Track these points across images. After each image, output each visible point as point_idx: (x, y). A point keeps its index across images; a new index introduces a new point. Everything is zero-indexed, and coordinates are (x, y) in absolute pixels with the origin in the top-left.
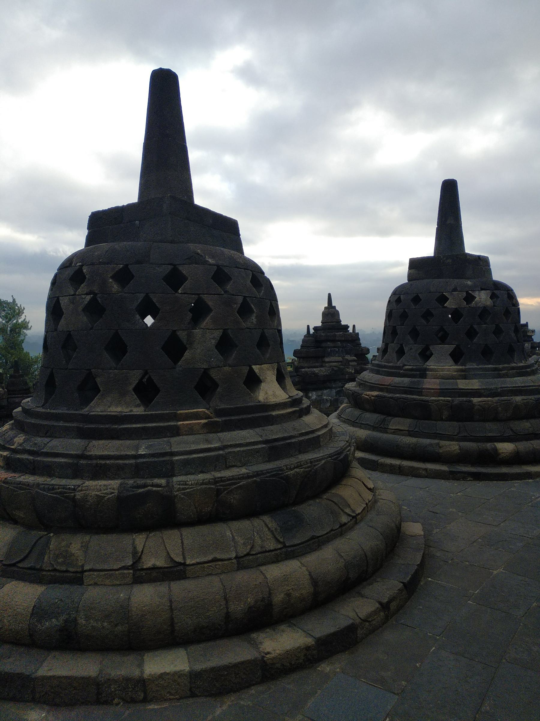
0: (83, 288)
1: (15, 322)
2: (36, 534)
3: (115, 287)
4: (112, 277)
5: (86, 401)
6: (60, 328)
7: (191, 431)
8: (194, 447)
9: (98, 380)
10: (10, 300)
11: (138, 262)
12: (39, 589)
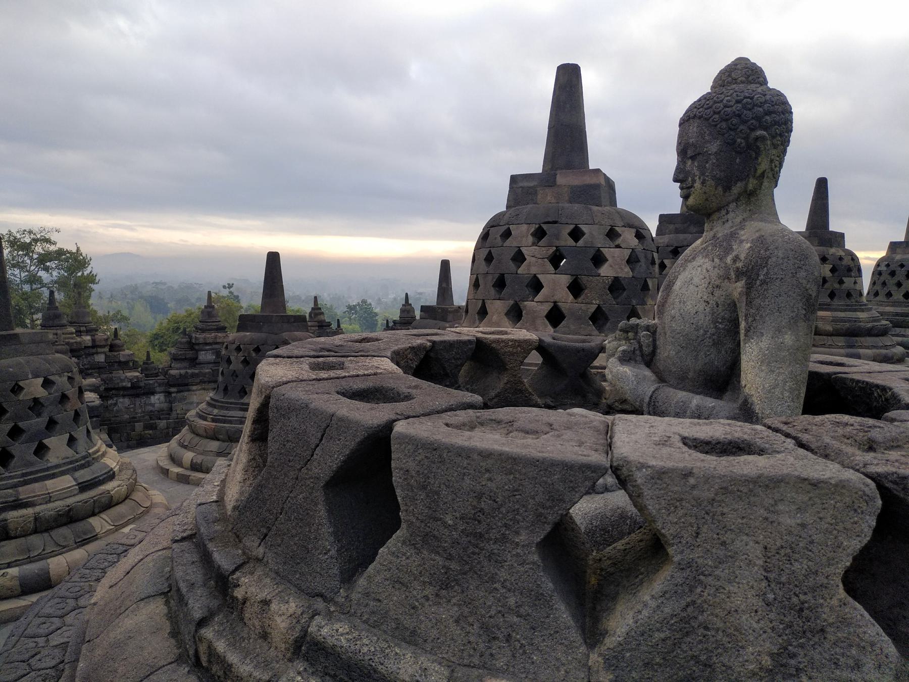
0: (241, 354)
1: (79, 274)
2: (226, 444)
3: (254, 354)
4: (253, 350)
5: (242, 397)
6: (230, 368)
9: (247, 389)
10: (74, 250)
11: (263, 345)
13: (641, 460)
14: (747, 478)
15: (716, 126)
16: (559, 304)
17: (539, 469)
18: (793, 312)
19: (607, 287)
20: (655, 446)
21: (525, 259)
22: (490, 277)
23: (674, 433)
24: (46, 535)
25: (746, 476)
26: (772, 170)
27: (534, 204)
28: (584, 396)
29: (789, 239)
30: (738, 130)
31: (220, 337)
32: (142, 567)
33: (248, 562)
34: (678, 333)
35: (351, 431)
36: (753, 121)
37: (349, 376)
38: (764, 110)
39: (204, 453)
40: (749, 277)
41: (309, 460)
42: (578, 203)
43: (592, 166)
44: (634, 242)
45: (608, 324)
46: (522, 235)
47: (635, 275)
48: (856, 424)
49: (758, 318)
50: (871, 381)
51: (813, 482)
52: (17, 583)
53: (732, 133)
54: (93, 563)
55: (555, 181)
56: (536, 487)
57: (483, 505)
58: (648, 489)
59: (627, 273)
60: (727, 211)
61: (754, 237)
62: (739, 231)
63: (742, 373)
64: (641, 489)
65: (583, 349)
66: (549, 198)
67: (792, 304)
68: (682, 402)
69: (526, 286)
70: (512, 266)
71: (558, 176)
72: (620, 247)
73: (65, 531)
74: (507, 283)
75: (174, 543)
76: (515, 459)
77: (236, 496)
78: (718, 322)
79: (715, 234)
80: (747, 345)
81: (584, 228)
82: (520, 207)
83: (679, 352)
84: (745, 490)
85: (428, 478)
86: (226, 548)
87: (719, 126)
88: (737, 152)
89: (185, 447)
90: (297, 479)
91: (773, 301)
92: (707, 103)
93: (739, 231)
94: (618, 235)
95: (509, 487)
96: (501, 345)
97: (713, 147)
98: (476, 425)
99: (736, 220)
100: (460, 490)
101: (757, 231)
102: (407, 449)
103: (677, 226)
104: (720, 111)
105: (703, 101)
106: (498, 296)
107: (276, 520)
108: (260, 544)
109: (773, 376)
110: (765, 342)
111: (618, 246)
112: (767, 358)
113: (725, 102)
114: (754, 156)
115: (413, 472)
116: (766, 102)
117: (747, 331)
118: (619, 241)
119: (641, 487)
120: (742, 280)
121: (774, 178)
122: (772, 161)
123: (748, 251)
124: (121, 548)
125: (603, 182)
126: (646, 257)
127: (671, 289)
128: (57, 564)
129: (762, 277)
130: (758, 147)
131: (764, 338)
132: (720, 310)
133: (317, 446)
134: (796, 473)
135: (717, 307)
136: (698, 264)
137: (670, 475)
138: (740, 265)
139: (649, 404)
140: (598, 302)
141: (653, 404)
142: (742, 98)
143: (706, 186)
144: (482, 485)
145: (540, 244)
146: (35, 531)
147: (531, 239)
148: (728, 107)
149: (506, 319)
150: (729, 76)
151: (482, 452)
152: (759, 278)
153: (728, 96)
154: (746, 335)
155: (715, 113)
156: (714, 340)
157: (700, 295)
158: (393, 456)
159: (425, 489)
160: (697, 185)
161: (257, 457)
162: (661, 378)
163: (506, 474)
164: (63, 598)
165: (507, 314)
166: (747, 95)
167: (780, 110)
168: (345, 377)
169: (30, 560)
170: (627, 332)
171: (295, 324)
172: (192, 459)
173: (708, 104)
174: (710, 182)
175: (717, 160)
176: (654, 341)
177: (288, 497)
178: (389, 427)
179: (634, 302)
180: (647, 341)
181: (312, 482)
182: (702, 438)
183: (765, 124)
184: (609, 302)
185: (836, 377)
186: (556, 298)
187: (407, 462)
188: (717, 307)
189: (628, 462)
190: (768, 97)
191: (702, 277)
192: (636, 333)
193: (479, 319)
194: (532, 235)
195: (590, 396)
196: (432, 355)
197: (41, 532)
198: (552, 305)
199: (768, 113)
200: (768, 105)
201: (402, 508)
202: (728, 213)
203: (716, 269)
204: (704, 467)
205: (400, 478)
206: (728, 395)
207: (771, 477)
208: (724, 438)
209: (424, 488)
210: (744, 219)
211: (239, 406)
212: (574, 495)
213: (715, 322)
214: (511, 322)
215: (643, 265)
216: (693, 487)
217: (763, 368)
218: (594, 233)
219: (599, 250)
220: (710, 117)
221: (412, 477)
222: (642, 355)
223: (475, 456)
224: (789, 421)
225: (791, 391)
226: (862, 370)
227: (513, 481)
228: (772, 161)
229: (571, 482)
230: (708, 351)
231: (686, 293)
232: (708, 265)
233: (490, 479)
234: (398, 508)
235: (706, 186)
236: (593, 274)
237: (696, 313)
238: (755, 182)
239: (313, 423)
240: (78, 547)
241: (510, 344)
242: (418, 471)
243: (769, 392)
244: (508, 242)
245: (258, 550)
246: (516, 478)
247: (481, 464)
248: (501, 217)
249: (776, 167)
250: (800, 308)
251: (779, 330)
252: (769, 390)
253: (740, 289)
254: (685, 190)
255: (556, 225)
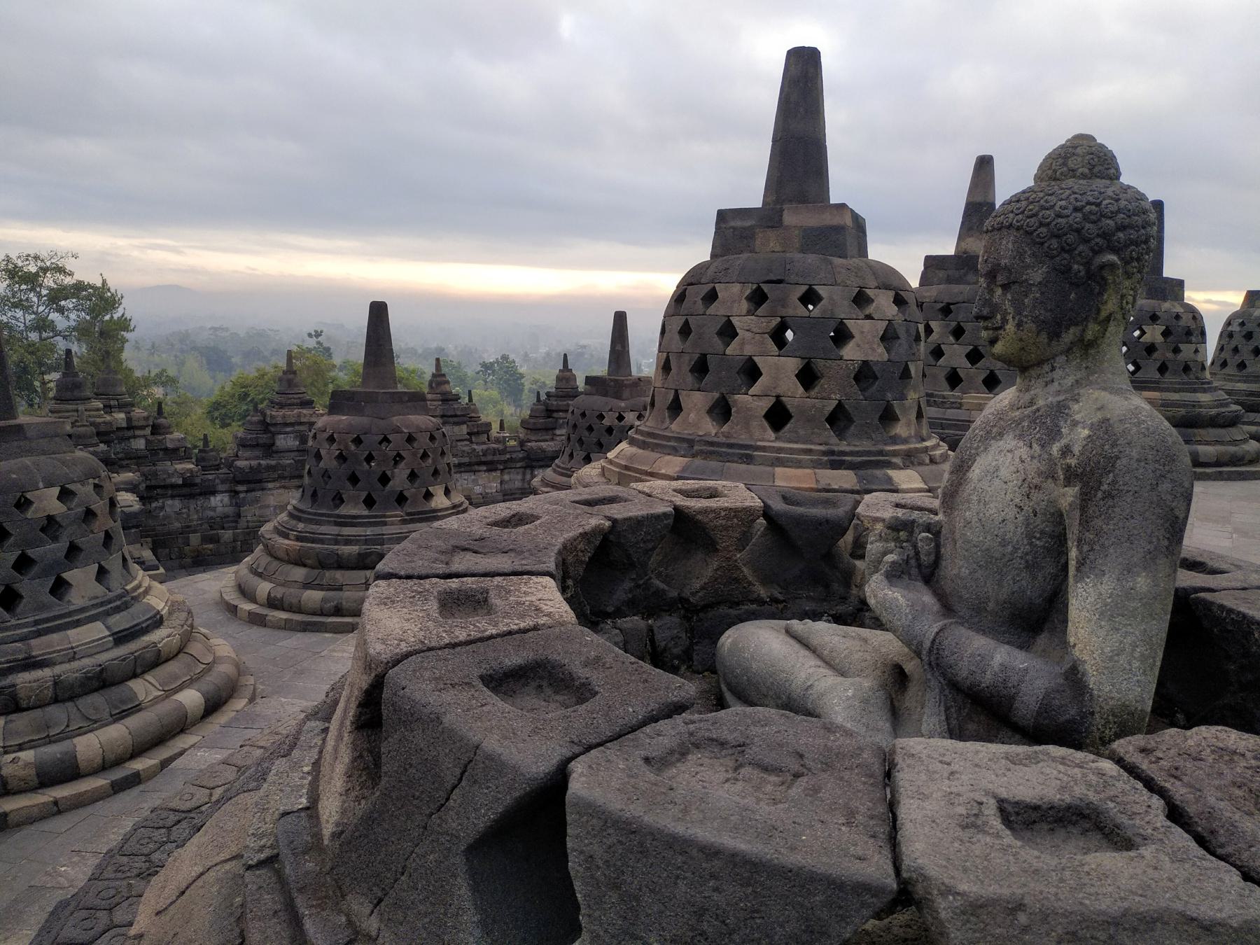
1: (107, 318)
2: (316, 571)
3: (353, 447)
4: (352, 441)
5: (337, 507)
7: (392, 523)
8: (394, 532)
9: (343, 496)
10: (99, 284)
12: (323, 593)
13: (947, 881)
14: (1105, 918)
15: (1042, 244)
16: (783, 399)
17: (792, 883)
18: (1150, 543)
19: (852, 375)
20: (959, 832)
21: (737, 334)
22: (686, 358)
23: (987, 793)
24: (69, 704)
25: (1104, 913)
26: (1122, 309)
27: (751, 252)
28: (827, 586)
29: (1148, 429)
30: (1077, 252)
31: (305, 415)
32: (201, 892)
33: (355, 940)
34: (976, 547)
35: (505, 779)
36: (1098, 240)
37: (498, 635)
38: (1116, 223)
39: (284, 584)
40: (1085, 485)
41: (442, 805)
42: (814, 253)
43: (834, 200)
44: (892, 310)
45: (852, 428)
46: (733, 298)
47: (892, 358)
48: (1248, 755)
49: (1097, 547)
50: (1251, 613)
51: (1205, 923)
52: (33, 772)
53: (1066, 256)
54: (132, 846)
55: (781, 220)
56: (786, 909)
57: (705, 926)
58: (957, 929)
59: (880, 355)
60: (1053, 367)
61: (1095, 420)
62: (1070, 404)
63: (1070, 624)
64: (946, 927)
65: (827, 521)
66: (772, 244)
67: (1149, 531)
68: (979, 655)
69: (738, 373)
70: (717, 342)
71: (785, 213)
72: (873, 319)
73: (97, 699)
74: (711, 367)
75: (247, 869)
76: (754, 864)
77: (335, 818)
78: (1035, 537)
79: (1032, 399)
80: (1079, 585)
81: (822, 291)
82: (733, 257)
83: (975, 571)
84: (1102, 936)
85: (623, 872)
86: (323, 910)
87: (1046, 245)
88: (1071, 284)
89: (260, 575)
90: (425, 828)
91: (1121, 524)
92: (1030, 207)
93: (1070, 404)
94: (869, 301)
95: (746, 905)
96: (710, 516)
97: (1037, 275)
98: (689, 749)
99: (1066, 381)
100: (671, 900)
101: (1099, 409)
102: (591, 823)
103: (950, 272)
104: (1049, 224)
105: (1024, 203)
106: (697, 386)
107: (396, 880)
108: (372, 912)
109: (1117, 636)
110: (1107, 586)
111: (869, 317)
112: (1109, 610)
113: (1057, 208)
114: (1097, 291)
115: (600, 861)
116: (1119, 211)
117: (1081, 564)
118: (870, 309)
119: (946, 924)
120: (1076, 486)
121: (1124, 319)
122: (1123, 297)
123: (1085, 443)
124: (173, 818)
125: (848, 221)
126: (907, 331)
127: (965, 474)
128: (88, 746)
129: (1105, 487)
130: (1103, 278)
131: (1105, 579)
132: (1038, 521)
133: (454, 787)
134: (1179, 906)
135: (1035, 516)
136: (1009, 447)
137: (990, 909)
138: (1073, 462)
139: (930, 651)
140: (838, 397)
141: (935, 652)
142: (1083, 204)
143: (1022, 330)
144: (705, 897)
145: (758, 312)
146: (56, 700)
147: (745, 305)
148: (1062, 217)
149: (708, 419)
150: (1064, 164)
151: (705, 847)
152: (1102, 488)
153: (1061, 200)
154: (1078, 569)
155: (1041, 225)
156: (1027, 562)
157: (1009, 497)
158: (569, 831)
159: (619, 888)
160: (1010, 327)
161: (365, 754)
162: (947, 608)
163: (742, 885)
164: (91, 909)
165: (710, 411)
166: (1091, 199)
167: (1140, 223)
168: (491, 637)
169: (50, 740)
170: (898, 531)
171: (409, 404)
172: (269, 592)
173: (1031, 210)
174: (1031, 326)
175: (1042, 293)
176: (938, 546)
177: (413, 852)
178: (560, 778)
179: (889, 396)
180: (927, 548)
181: (447, 841)
182: (1028, 800)
183: (1116, 244)
184: (854, 397)
185: (1198, 598)
186: (779, 391)
187: (591, 844)
188: (1035, 516)
189: (926, 878)
190: (1123, 203)
191: (1013, 469)
192: (911, 533)
193: (669, 417)
194: (746, 298)
195: (835, 586)
196: (612, 537)
197: (63, 701)
198: (774, 400)
199: (1122, 228)
200: (1122, 215)
201: (583, 912)
202: (1053, 369)
203: (1035, 461)
204: (1041, 893)
205: (580, 865)
206: (1042, 640)
207: (1141, 914)
208: (1059, 800)
209: (616, 887)
210: (1077, 381)
211: (332, 519)
212: (845, 928)
213: (1030, 536)
214: (715, 423)
215: (902, 347)
216: (1025, 929)
217: (1103, 623)
218: (835, 297)
219: (842, 323)
220: (1035, 230)
221: (598, 867)
222: (919, 566)
223: (694, 852)
224: (1149, 747)
225: (1143, 658)
226: (1234, 584)
227: (751, 898)
228: (1123, 297)
229: (840, 907)
230: (1018, 575)
231: (989, 489)
232: (1023, 451)
233: (716, 890)
234: (577, 907)
235: (1022, 330)
236: (833, 357)
237: (1004, 521)
238: (1097, 328)
239: (447, 751)
240: (115, 721)
241: (723, 514)
242: (607, 861)
243: (1111, 659)
244: (712, 309)
245: (369, 922)
246: (756, 892)
247: (704, 865)
248: (704, 269)
249: (1127, 303)
250: (1161, 537)
251: (1129, 570)
252: (1111, 657)
253: (1072, 499)
254: (991, 332)
255: (782, 285)
